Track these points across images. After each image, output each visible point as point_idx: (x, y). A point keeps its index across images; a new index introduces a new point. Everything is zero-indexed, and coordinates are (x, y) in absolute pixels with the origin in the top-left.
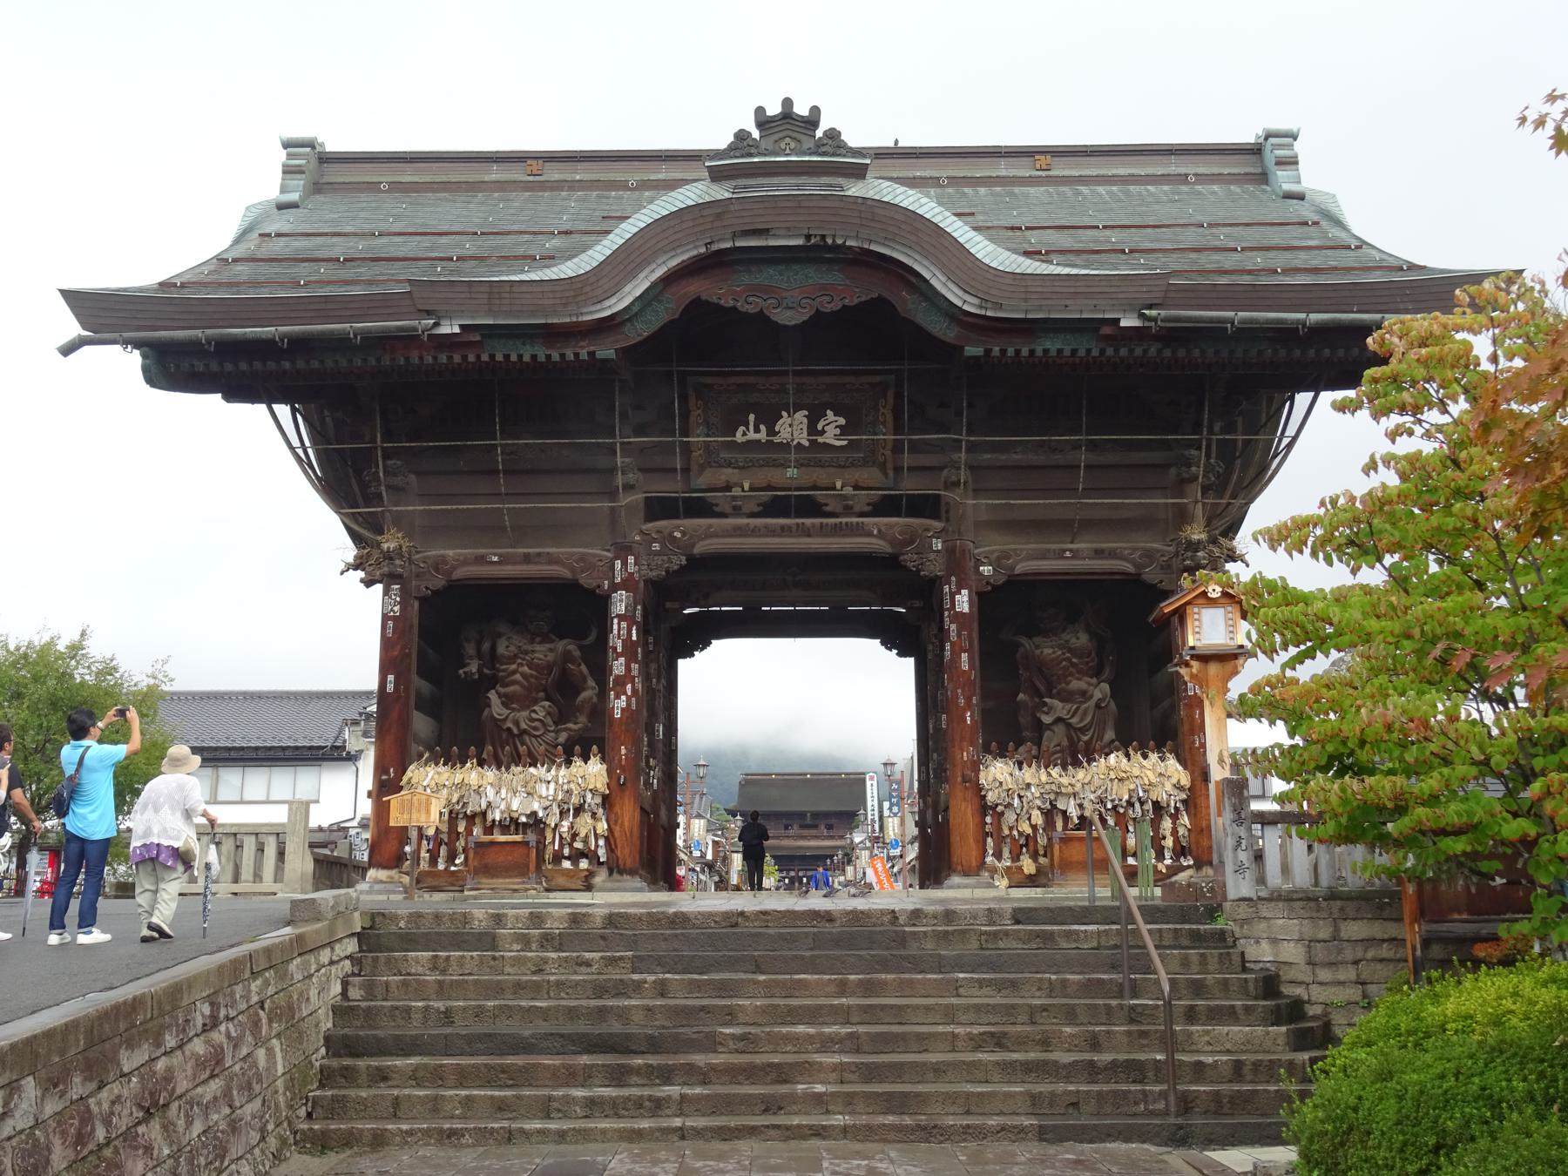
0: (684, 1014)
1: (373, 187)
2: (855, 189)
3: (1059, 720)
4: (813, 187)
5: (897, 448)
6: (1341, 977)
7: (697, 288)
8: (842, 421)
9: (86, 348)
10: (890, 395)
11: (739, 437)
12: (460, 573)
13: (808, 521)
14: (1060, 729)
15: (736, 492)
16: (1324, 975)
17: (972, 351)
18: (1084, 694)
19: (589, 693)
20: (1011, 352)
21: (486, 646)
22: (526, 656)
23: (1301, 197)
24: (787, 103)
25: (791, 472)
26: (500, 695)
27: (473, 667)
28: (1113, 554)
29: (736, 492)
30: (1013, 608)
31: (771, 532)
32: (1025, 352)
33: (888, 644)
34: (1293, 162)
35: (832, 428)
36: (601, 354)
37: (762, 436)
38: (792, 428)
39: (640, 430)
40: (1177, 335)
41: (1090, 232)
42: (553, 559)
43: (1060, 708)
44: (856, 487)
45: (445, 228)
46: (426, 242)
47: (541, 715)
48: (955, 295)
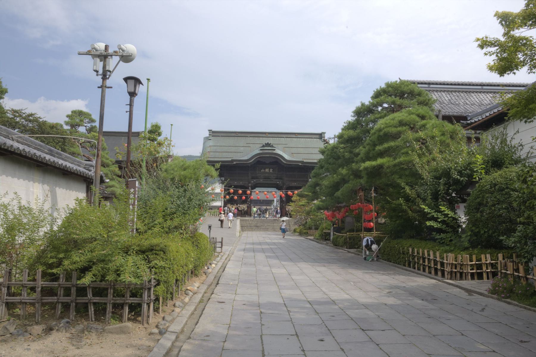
2: (274, 152)
4: (270, 151)
7: (259, 159)
35: (271, 170)
38: (267, 170)
48: (284, 161)
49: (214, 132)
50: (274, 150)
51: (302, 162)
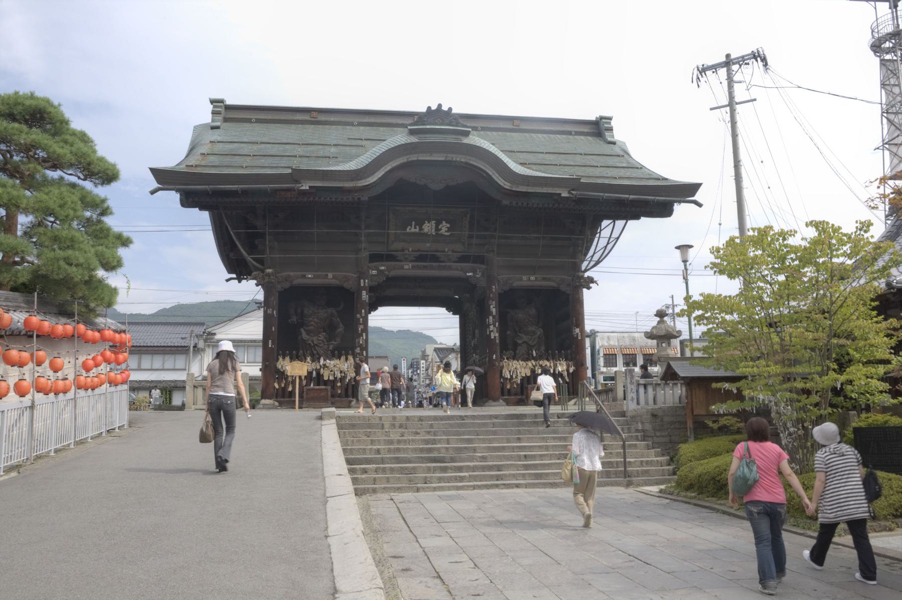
0: (459, 450)
1: (249, 121)
2: (466, 141)
3: (525, 342)
4: (450, 139)
5: (471, 237)
6: (663, 434)
8: (448, 225)
9: (160, 192)
10: (468, 216)
11: (408, 230)
12: (296, 282)
13: (434, 264)
14: (525, 345)
15: (406, 252)
16: (658, 434)
17: (506, 202)
18: (534, 333)
19: (341, 329)
20: (520, 204)
21: (299, 311)
22: (316, 315)
23: (614, 143)
24: (440, 106)
25: (428, 245)
26: (305, 330)
27: (294, 319)
28: (549, 280)
29: (406, 252)
30: (510, 300)
31: (419, 268)
32: (525, 204)
33: (449, 309)
34: (611, 129)
35: (444, 227)
36: (362, 199)
37: (417, 230)
39: (367, 227)
40: (580, 201)
41: (541, 155)
42: (330, 278)
43: (525, 338)
44: (453, 251)
45: (285, 141)
46: (281, 147)
47: (322, 338)
49: (229, 108)
50: (467, 134)
51: (573, 183)
